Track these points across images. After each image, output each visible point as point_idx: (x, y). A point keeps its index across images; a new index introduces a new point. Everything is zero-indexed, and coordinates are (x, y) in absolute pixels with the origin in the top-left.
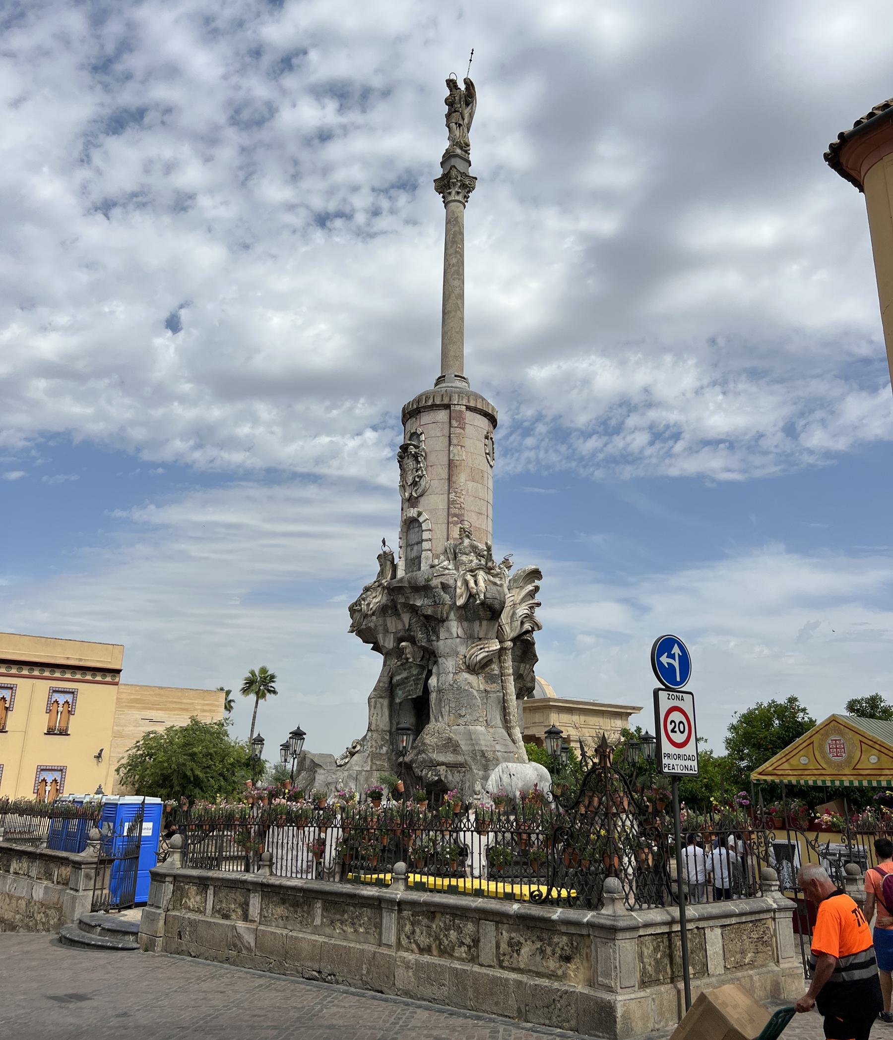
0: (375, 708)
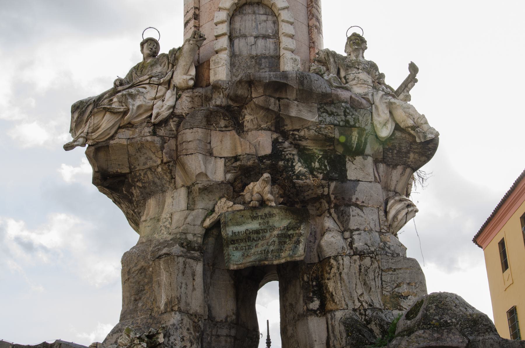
0: (183, 273)
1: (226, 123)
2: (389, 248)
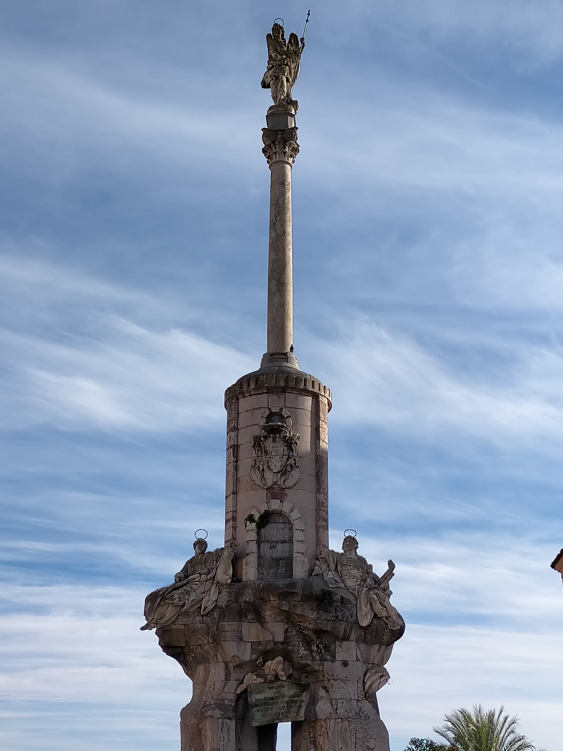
0: (222, 731)
1: (252, 617)
2: (363, 713)
